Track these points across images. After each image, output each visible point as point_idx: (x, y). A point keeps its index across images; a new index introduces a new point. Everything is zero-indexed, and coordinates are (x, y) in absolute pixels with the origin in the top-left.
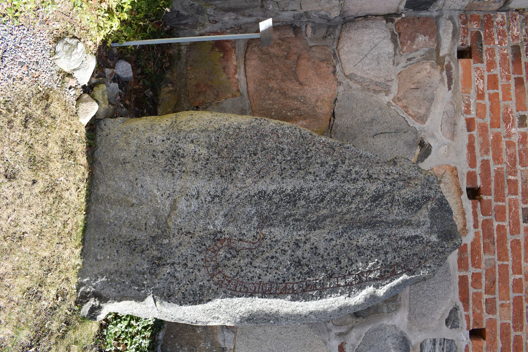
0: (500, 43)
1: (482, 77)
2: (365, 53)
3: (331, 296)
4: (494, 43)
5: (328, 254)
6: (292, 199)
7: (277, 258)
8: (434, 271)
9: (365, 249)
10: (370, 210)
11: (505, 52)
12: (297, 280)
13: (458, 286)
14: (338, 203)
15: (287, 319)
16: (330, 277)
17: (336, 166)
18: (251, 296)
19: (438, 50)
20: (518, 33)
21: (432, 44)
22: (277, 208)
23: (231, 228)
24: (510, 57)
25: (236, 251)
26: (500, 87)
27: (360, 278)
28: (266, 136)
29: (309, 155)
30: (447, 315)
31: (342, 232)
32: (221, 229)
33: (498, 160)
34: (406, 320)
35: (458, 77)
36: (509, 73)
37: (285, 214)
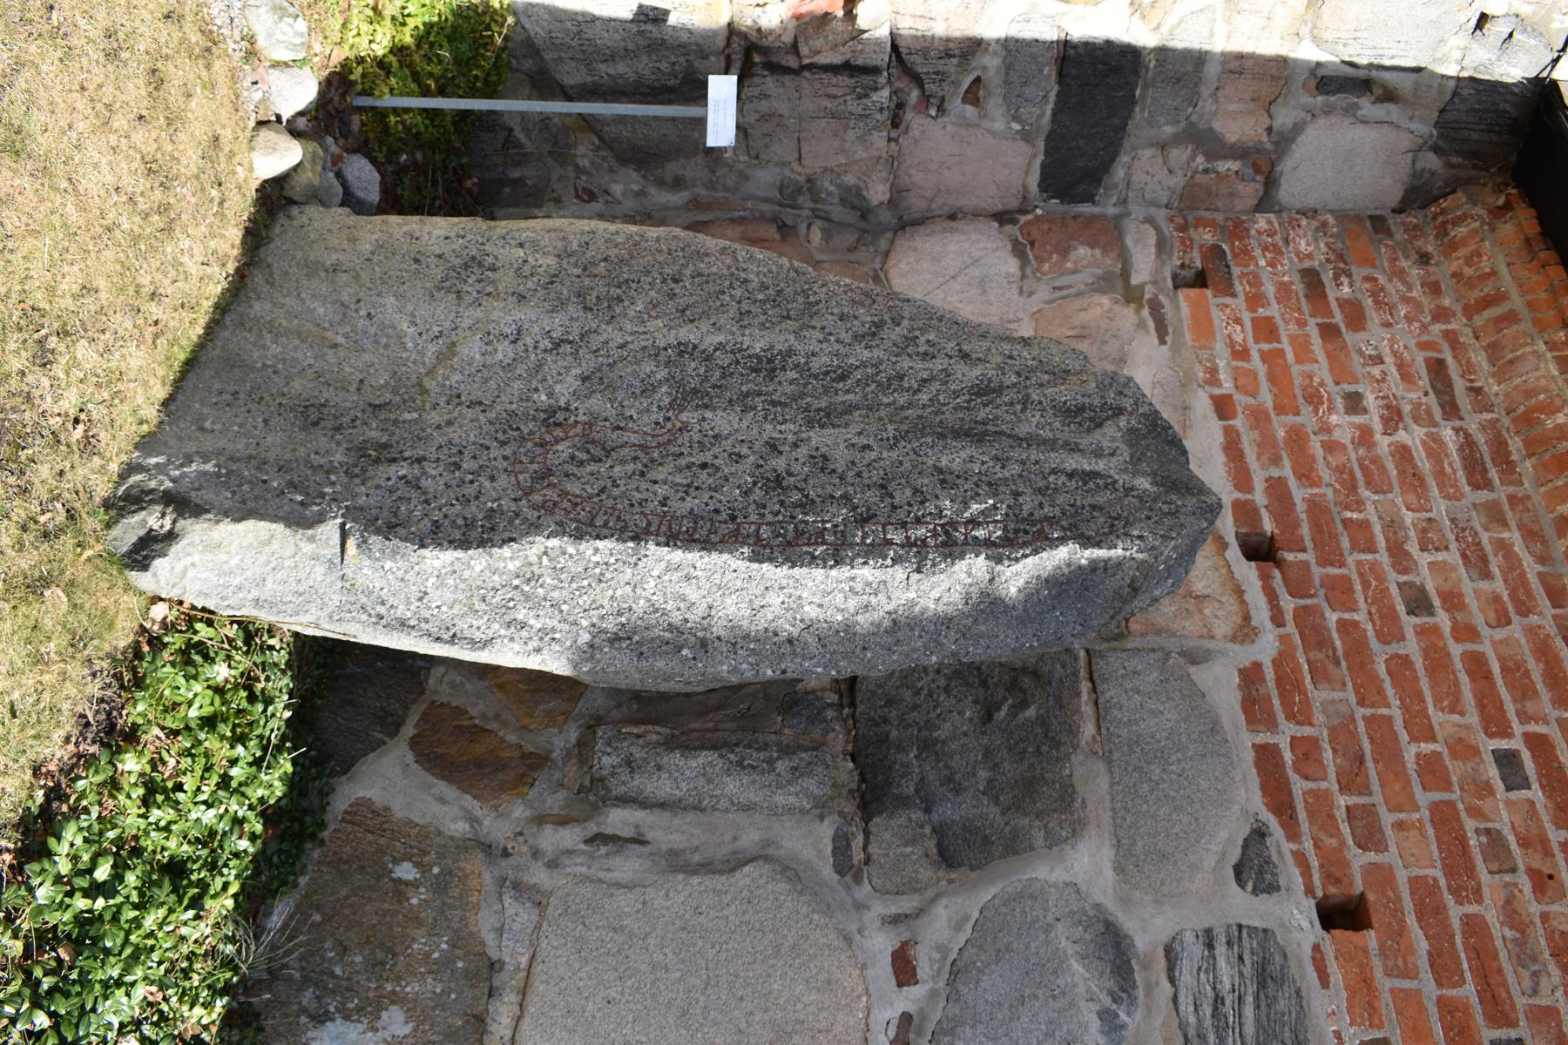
0: (1271, 264)
1: (1238, 321)
2: (952, 272)
3: (865, 563)
4: (1257, 265)
5: (859, 474)
6: (768, 366)
7: (718, 469)
8: (1153, 548)
9: (958, 477)
10: (968, 409)
11: (1286, 279)
12: (770, 518)
13: (1254, 771)
14: (885, 387)
15: (734, 645)
16: (863, 521)
17: (879, 325)
18: (636, 538)
19: (1125, 274)
20: (1310, 249)
21: (1110, 262)
22: (723, 376)
23: (597, 403)
24: (1299, 287)
25: (603, 448)
26: (1285, 340)
27: (947, 533)
28: (707, 255)
29: (812, 299)
30: (1235, 854)
31: (895, 437)
32: (568, 404)
33: (1308, 478)
34: (1109, 873)
35: (1180, 320)
36: (1301, 313)
37: (744, 388)
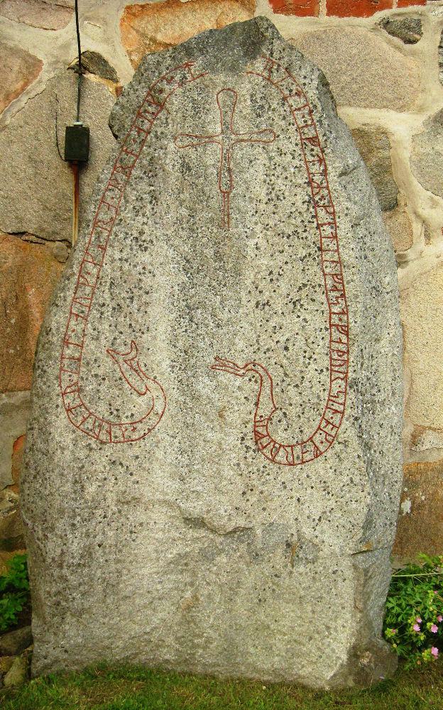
13: (345, 18)
30: (397, 41)
34: (404, 116)
